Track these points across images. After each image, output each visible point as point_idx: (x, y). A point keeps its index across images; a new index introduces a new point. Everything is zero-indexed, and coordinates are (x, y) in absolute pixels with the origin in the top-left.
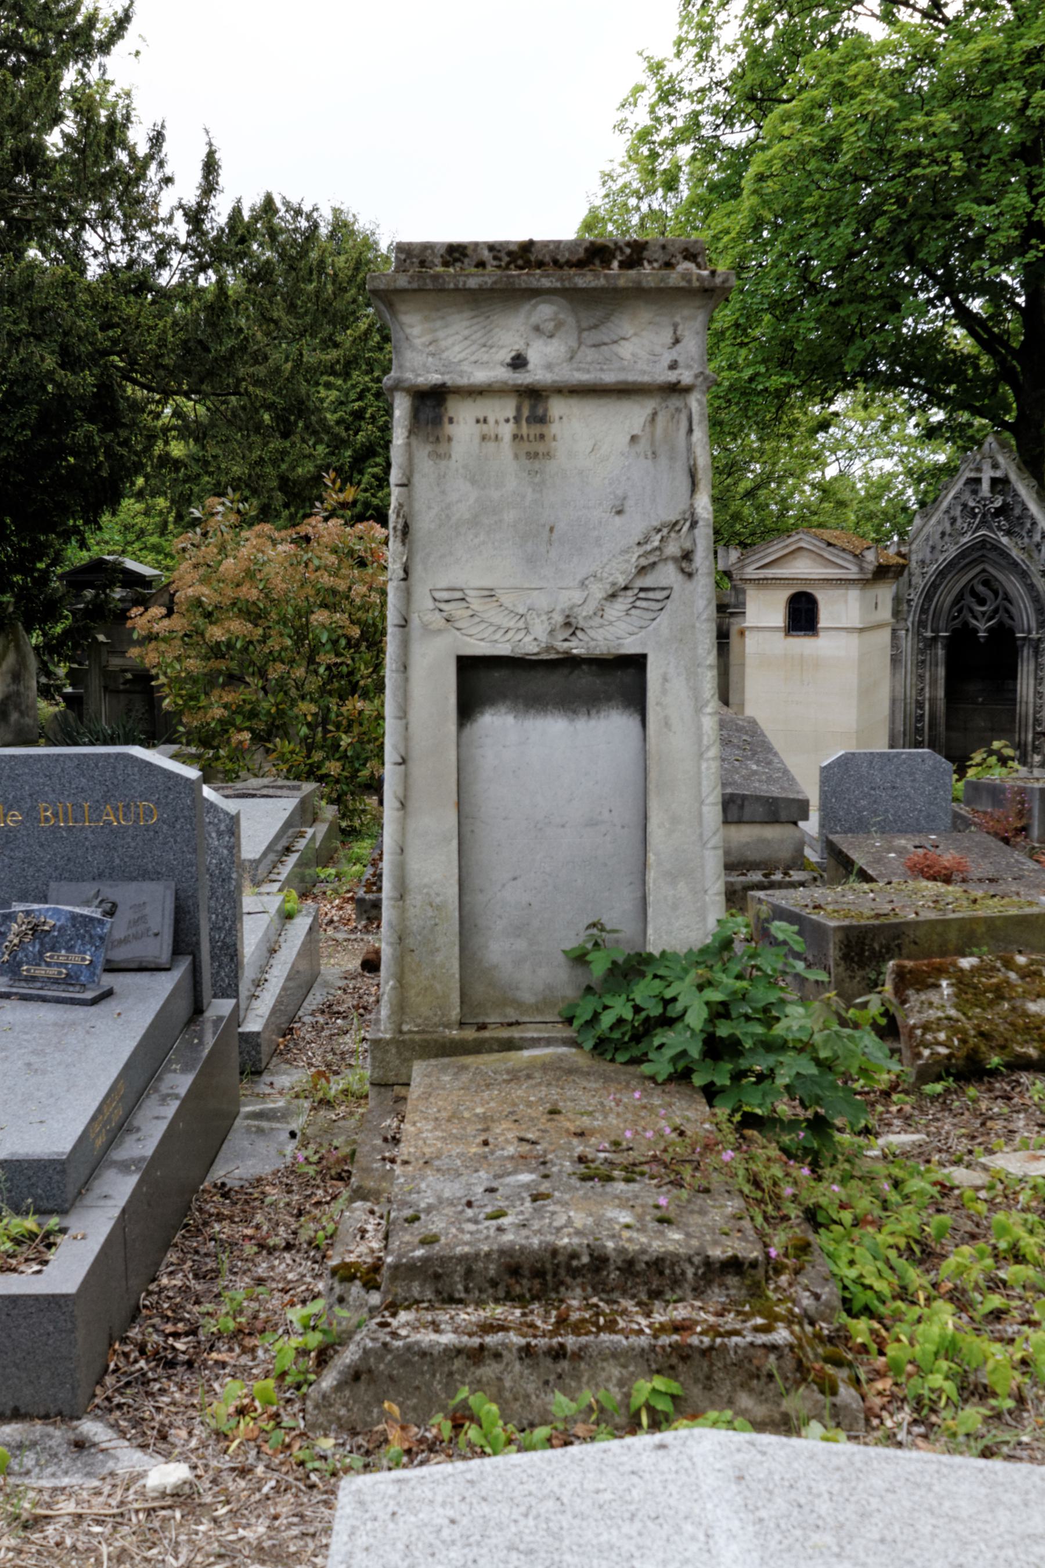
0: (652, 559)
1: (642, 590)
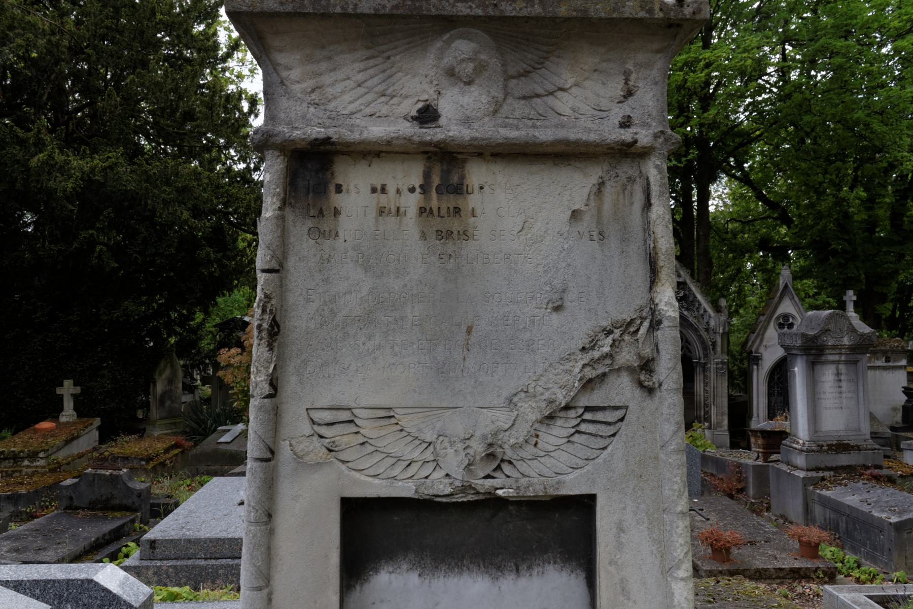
0: (601, 369)
1: (588, 409)
